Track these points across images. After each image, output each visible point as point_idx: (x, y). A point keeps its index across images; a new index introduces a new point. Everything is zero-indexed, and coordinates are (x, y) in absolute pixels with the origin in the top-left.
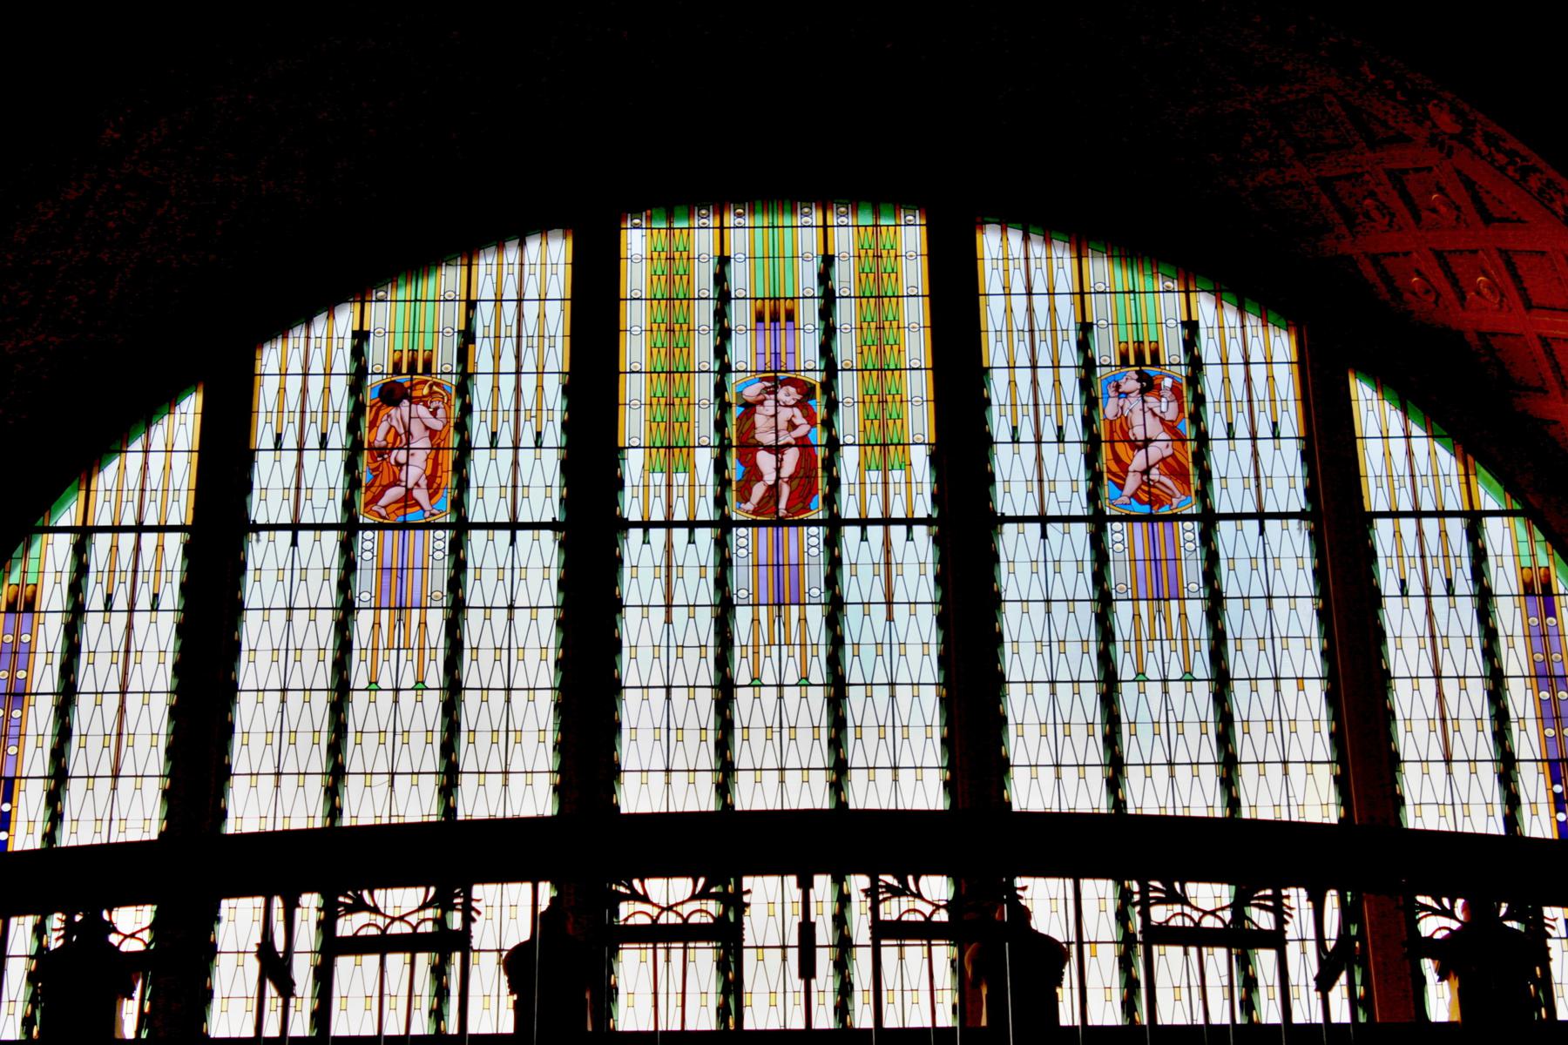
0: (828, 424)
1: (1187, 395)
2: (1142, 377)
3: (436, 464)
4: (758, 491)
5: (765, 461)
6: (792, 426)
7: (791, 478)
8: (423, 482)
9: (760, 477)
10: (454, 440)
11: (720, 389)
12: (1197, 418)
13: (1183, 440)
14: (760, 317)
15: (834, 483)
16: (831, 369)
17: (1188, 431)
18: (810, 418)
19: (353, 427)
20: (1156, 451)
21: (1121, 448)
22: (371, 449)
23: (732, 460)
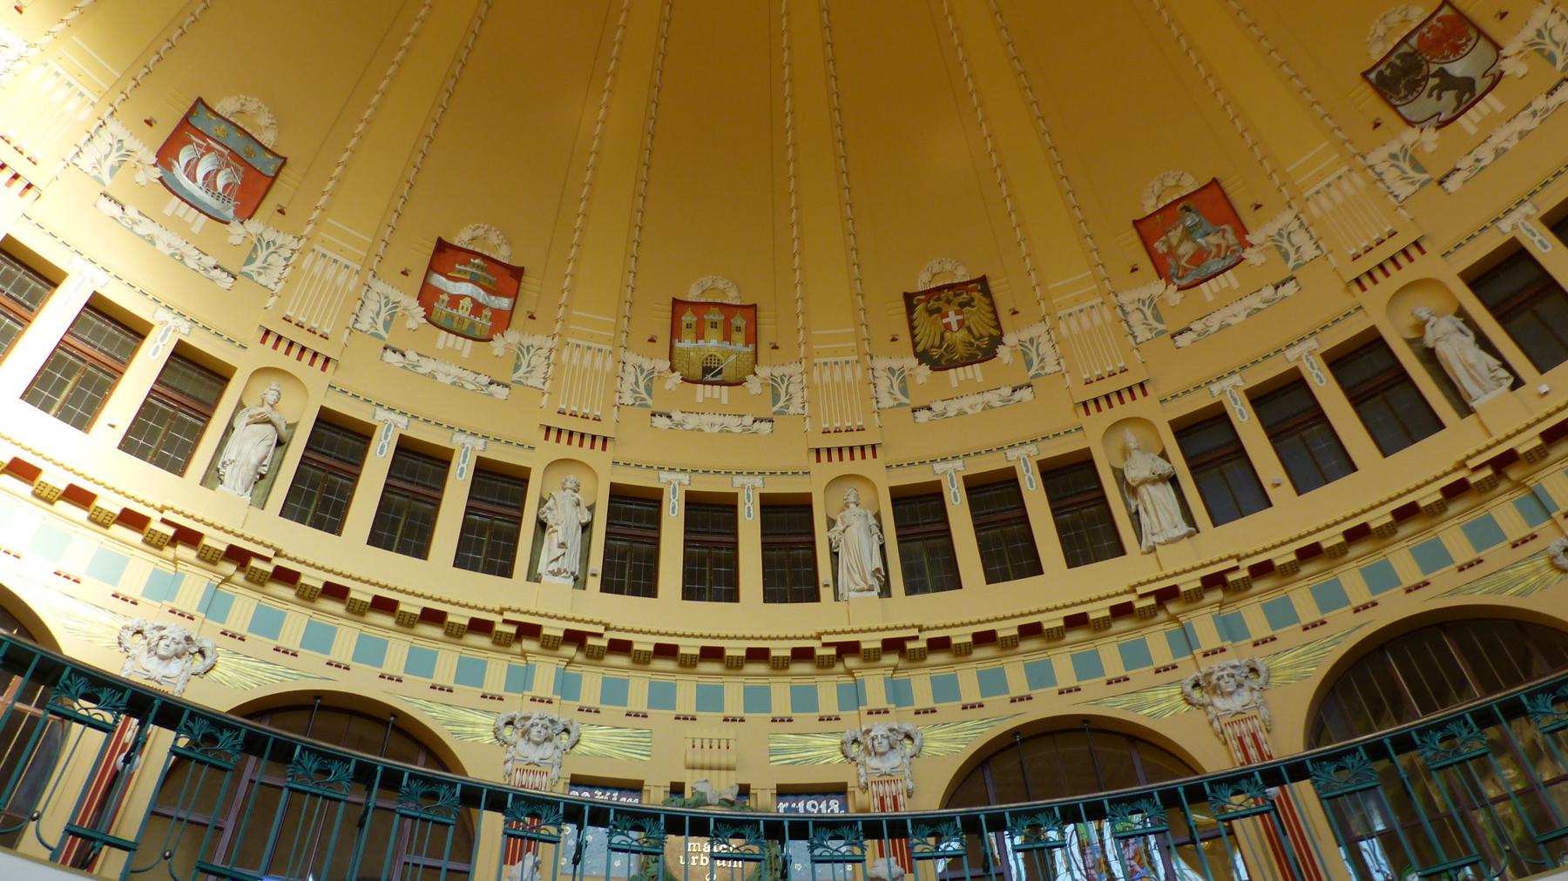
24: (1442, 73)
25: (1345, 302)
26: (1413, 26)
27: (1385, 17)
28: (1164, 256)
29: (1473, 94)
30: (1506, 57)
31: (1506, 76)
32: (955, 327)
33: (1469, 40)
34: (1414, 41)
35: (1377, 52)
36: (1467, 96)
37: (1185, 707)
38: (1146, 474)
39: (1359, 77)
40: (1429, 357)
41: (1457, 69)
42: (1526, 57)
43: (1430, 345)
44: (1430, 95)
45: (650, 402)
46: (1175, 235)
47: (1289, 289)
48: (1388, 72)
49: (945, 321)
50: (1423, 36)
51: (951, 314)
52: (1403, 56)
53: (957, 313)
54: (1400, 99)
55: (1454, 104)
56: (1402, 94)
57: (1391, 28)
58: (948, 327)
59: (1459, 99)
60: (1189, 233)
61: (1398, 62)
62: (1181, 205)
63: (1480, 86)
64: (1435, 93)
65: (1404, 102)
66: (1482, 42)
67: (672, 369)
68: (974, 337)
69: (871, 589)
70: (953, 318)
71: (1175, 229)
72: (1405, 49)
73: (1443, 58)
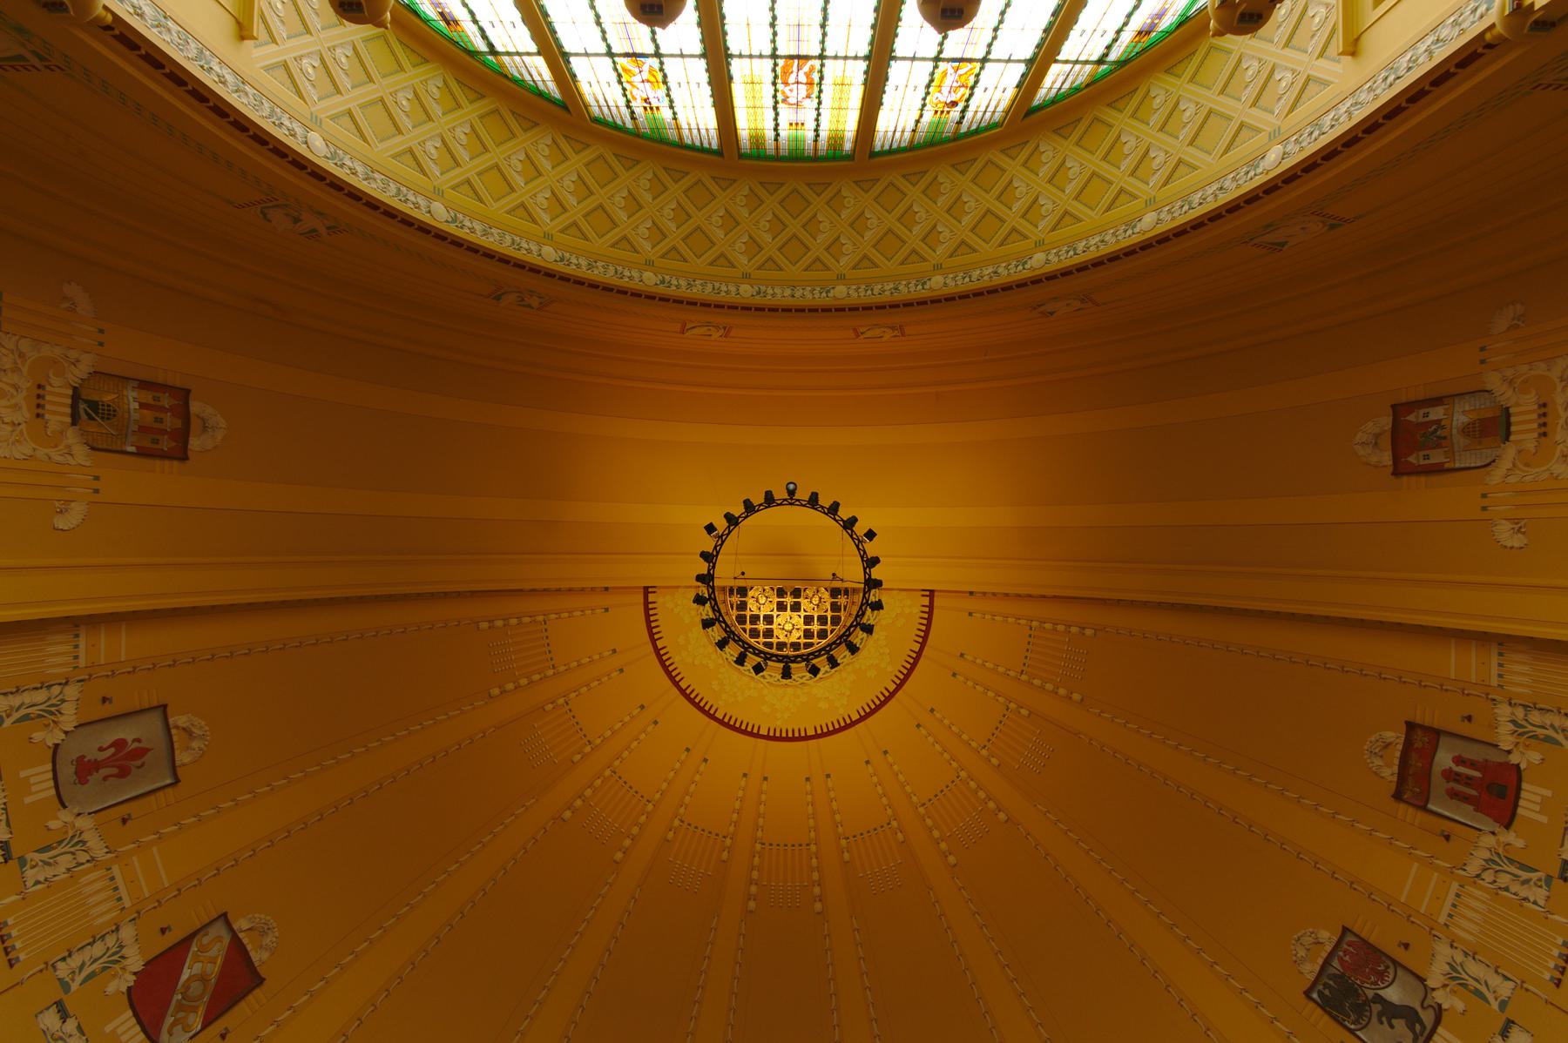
0: (776, 91)
1: (629, 97)
2: (650, 103)
3: (941, 82)
4: (806, 69)
5: (803, 79)
6: (791, 91)
7: (792, 72)
8: (948, 75)
9: (805, 73)
10: (931, 89)
11: (820, 103)
12: (624, 89)
13: (628, 82)
14: (803, 124)
15: (774, 70)
16: (775, 108)
17: (625, 85)
18: (783, 93)
19: (971, 95)
20: (638, 79)
21: (652, 79)
22: (967, 87)
23: (817, 80)
24: (1379, 999)
26: (1329, 949)
27: (1299, 939)
29: (1423, 1027)
30: (1433, 989)
31: (1445, 1010)
33: (1388, 967)
34: (1336, 963)
35: (1310, 970)
36: (1418, 1027)
41: (1393, 994)
42: (1455, 992)
44: (1382, 1023)
48: (1327, 992)
50: (1341, 959)
52: (1333, 977)
54: (1353, 1023)
55: (1411, 1035)
56: (1352, 1017)
57: (1308, 950)
59: (1412, 1029)
61: (1331, 983)
63: (1427, 1017)
64: (1384, 1019)
65: (1359, 1026)
66: (1400, 972)
72: (1331, 971)
73: (1372, 983)
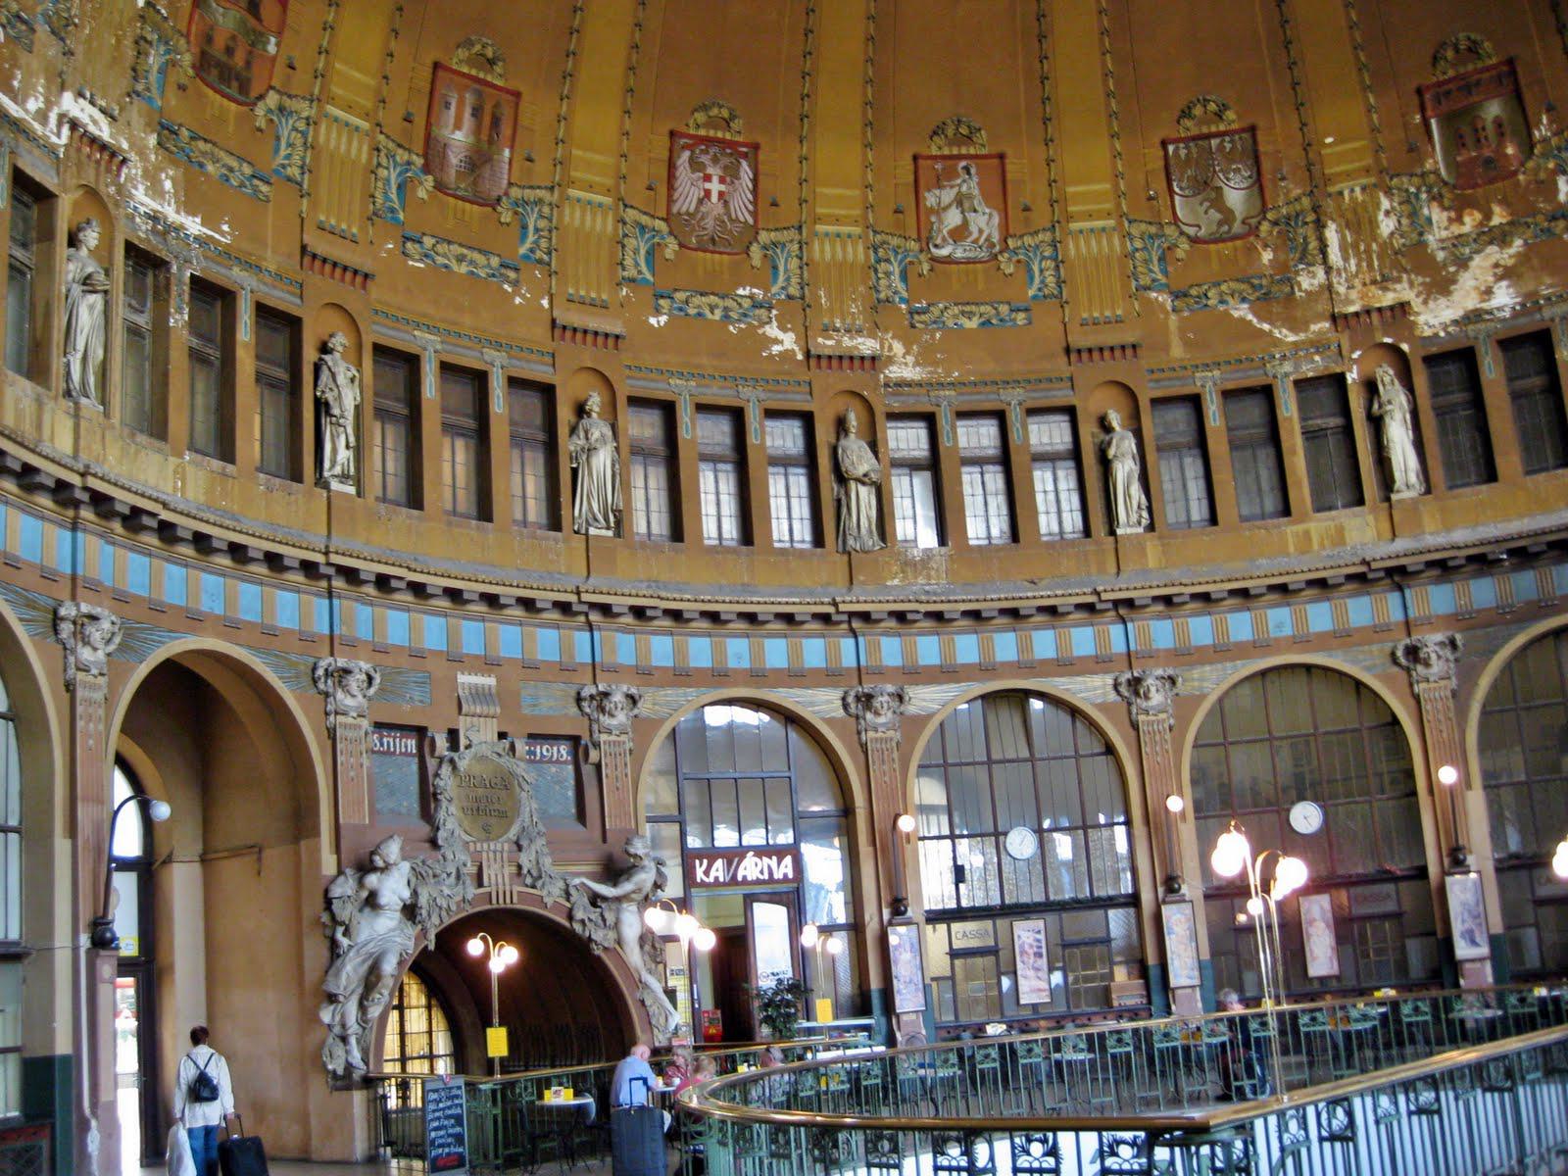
25: (1061, 364)
28: (931, 211)
32: (714, 197)
34: (1214, 142)
36: (1226, 228)
37: (841, 713)
38: (861, 469)
39: (1157, 141)
40: (1105, 464)
43: (1110, 457)
45: (401, 216)
46: (948, 195)
47: (1021, 318)
49: (707, 185)
51: (715, 179)
53: (722, 181)
54: (1181, 189)
58: (708, 193)
59: (1220, 223)
60: (959, 201)
62: (963, 163)
67: (427, 169)
68: (730, 219)
69: (608, 528)
70: (715, 187)
71: (952, 187)
